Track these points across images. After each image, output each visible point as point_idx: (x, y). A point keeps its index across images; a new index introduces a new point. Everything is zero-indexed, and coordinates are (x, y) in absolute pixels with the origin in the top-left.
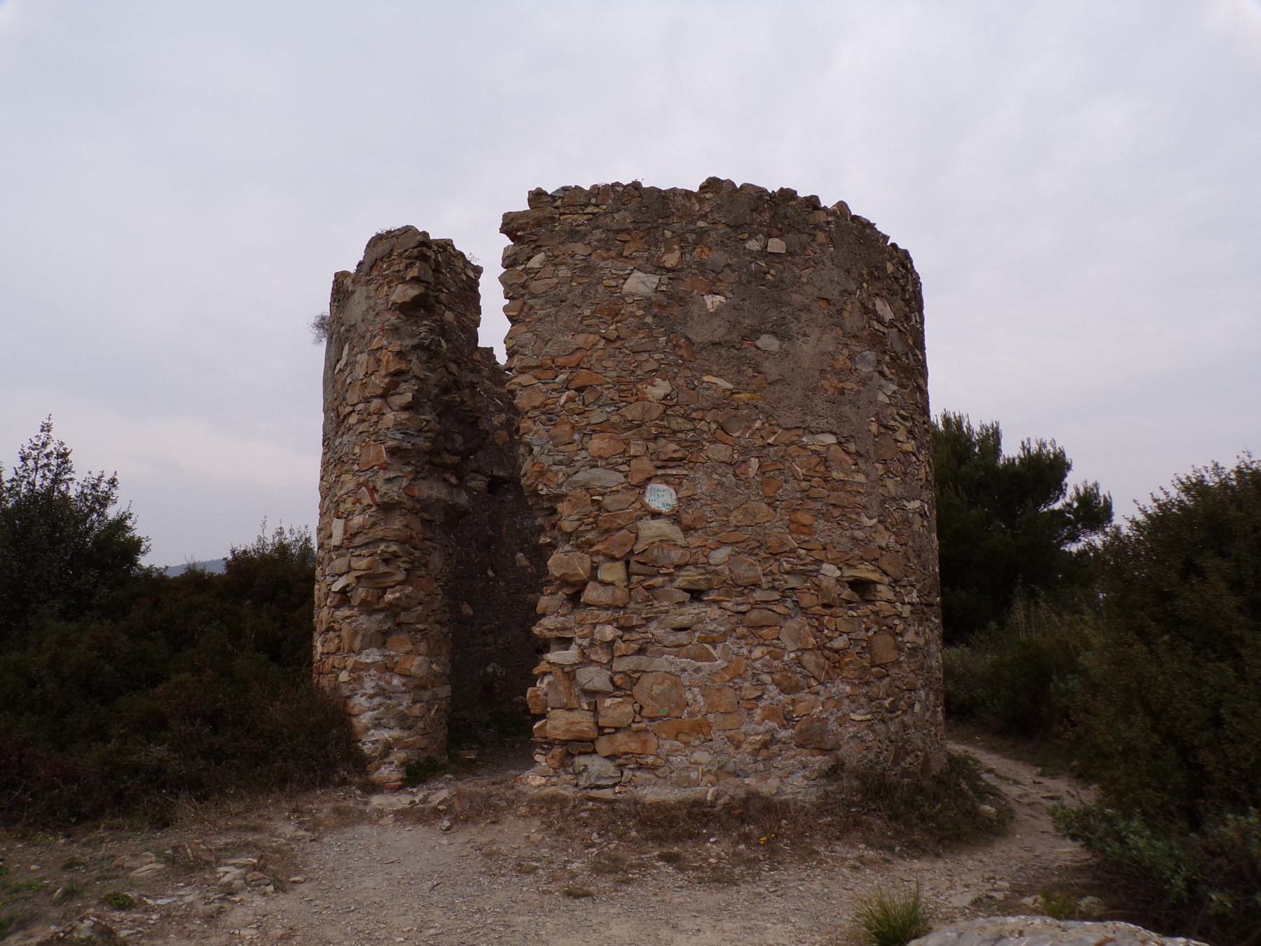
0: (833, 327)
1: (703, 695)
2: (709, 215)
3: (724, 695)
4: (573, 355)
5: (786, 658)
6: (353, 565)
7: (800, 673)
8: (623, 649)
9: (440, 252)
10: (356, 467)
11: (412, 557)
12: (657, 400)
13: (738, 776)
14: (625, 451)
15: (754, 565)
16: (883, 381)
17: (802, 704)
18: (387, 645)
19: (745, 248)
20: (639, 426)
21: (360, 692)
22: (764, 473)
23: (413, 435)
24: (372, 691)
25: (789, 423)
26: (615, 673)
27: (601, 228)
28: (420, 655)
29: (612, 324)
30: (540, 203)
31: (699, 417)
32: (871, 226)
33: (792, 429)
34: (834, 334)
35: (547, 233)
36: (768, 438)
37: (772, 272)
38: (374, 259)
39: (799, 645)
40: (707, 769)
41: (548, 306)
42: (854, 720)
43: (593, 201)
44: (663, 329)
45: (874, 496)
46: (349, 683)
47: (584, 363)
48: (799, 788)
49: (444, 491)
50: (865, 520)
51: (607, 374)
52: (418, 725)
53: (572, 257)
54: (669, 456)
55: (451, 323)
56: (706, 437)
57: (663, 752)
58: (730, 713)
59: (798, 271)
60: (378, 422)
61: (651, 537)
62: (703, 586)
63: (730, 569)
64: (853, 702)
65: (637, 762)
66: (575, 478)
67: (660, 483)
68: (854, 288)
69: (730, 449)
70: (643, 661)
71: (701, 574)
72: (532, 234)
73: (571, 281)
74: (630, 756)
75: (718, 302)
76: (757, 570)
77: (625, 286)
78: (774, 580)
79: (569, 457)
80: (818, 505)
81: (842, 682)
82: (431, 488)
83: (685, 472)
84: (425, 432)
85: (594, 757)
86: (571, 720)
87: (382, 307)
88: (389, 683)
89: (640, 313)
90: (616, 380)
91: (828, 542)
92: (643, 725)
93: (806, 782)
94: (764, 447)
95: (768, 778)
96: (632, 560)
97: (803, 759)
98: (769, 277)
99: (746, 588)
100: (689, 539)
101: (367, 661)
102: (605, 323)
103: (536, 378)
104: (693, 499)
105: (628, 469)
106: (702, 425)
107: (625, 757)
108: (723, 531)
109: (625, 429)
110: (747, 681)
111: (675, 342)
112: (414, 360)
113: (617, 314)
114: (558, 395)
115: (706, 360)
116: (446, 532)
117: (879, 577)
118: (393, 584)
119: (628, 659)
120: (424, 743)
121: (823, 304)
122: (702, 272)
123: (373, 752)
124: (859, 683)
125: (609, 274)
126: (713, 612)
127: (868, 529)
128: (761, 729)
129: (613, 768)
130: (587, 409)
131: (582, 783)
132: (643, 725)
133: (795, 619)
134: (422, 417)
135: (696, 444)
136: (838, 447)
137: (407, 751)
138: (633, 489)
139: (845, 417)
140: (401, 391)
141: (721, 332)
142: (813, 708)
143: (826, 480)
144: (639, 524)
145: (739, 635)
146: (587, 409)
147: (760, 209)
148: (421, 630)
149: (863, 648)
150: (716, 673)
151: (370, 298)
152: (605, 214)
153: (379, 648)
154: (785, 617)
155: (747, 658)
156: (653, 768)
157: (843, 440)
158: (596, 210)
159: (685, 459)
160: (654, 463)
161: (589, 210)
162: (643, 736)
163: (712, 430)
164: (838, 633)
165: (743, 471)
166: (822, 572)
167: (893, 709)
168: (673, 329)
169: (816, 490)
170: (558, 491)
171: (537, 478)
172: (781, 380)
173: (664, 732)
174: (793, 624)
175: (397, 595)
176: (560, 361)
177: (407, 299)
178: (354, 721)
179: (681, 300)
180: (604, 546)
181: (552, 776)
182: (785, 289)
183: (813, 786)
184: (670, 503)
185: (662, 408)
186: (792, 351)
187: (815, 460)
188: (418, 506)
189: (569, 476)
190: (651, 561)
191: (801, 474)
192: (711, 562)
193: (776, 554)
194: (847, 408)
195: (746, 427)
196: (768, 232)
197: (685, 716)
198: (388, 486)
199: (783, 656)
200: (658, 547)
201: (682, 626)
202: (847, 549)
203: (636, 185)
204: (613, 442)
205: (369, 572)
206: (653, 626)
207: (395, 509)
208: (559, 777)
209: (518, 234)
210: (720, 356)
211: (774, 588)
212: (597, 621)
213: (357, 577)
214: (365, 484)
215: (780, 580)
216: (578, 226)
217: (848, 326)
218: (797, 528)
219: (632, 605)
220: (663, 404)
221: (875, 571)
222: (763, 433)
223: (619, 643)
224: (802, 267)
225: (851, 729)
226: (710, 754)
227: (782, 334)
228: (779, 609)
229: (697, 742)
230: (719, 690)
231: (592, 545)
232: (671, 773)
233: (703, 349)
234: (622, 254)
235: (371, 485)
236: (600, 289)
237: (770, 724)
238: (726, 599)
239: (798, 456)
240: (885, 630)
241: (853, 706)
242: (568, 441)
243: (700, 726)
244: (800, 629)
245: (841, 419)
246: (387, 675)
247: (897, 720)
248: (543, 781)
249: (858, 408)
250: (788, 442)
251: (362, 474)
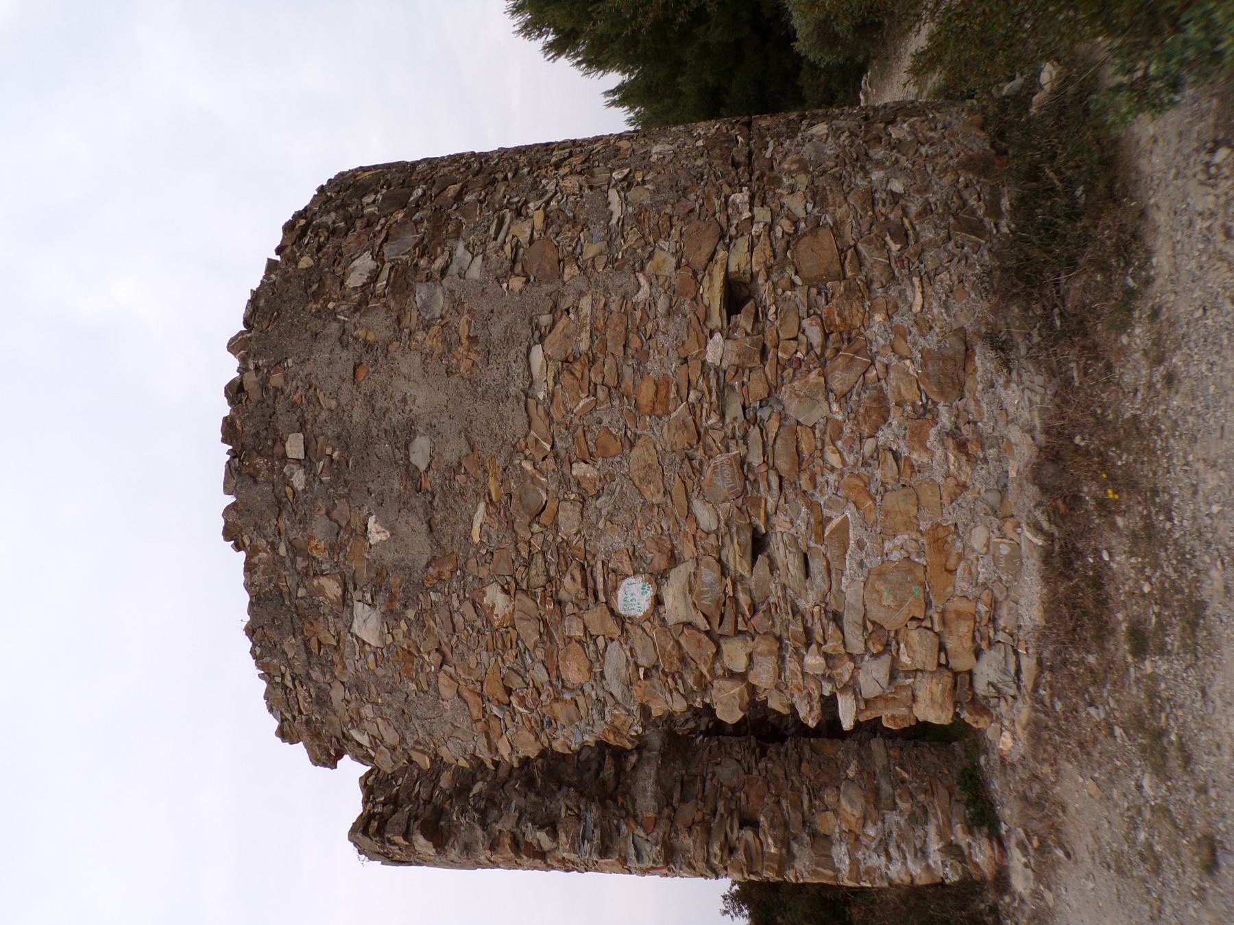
0: (389, 356)
1: (895, 536)
2: (270, 540)
3: (893, 506)
4: (468, 700)
5: (840, 417)
7: (859, 395)
8: (835, 644)
9: (374, 798)
11: (726, 815)
12: (511, 601)
13: (1006, 485)
14: (579, 642)
15: (715, 467)
16: (454, 269)
17: (903, 391)
18: (827, 833)
19: (304, 491)
20: (546, 624)
21: (884, 870)
22: (591, 455)
23: (584, 828)
24: (883, 859)
25: (521, 420)
26: (867, 649)
27: (308, 672)
28: (838, 800)
29: (423, 658)
31: (526, 547)
32: (256, 295)
33: (529, 416)
34: (398, 355)
36: (545, 450)
37: (329, 451)
39: (821, 397)
40: (996, 531)
42: (923, 306)
45: (608, 282)
48: (1023, 398)
49: (647, 769)
50: (642, 295)
53: (348, 702)
54: (580, 587)
55: (453, 774)
56: (551, 537)
57: (972, 592)
58: (918, 499)
59: (323, 414)
62: (747, 536)
63: (723, 502)
64: (896, 307)
65: (986, 625)
66: (619, 697)
67: (616, 598)
68: (335, 325)
69: (563, 504)
70: (851, 619)
73: (377, 704)
74: (977, 634)
75: (376, 525)
76: (722, 463)
77: (373, 644)
78: (733, 437)
79: (594, 704)
80: (628, 372)
81: (869, 327)
82: (645, 790)
83: (599, 565)
90: (491, 654)
91: (676, 355)
92: (936, 617)
93: (1013, 385)
94: (556, 457)
95: (1009, 440)
97: (980, 387)
98: (335, 455)
99: (746, 478)
102: (422, 666)
104: (634, 553)
105: (601, 638)
106: (537, 543)
108: (672, 513)
109: (551, 642)
110: (873, 474)
111: (435, 581)
113: (410, 653)
114: (518, 715)
115: (453, 539)
116: (694, 755)
117: (719, 265)
119: (848, 637)
120: (942, 792)
121: (361, 373)
122: (342, 547)
124: (869, 299)
125: (361, 662)
126: (781, 523)
127: (654, 291)
128: (939, 453)
129: (992, 652)
130: (531, 685)
131: (1012, 692)
132: (936, 617)
133: (786, 404)
134: (563, 815)
135: (563, 551)
136: (547, 340)
137: (953, 823)
138: (627, 631)
139: (505, 332)
141: (413, 520)
142: (908, 374)
143: (593, 361)
144: (671, 622)
145: (811, 486)
147: (252, 470)
148: (810, 800)
149: (819, 293)
150: (864, 518)
152: (290, 666)
153: (832, 844)
154: (783, 417)
155: (842, 475)
156: (994, 604)
157: (537, 334)
158: (288, 677)
159: (583, 565)
160: (592, 605)
161: (290, 684)
162: (950, 616)
163: (541, 529)
164: (801, 336)
165: (591, 485)
166: (718, 363)
167: (902, 235)
168: (418, 584)
169: (607, 376)
170: (637, 714)
172: (466, 433)
174: (793, 408)
175: (770, 841)
176: (476, 713)
177: (430, 844)
179: (381, 574)
181: (1002, 724)
182: (349, 433)
183: (1020, 375)
184: (641, 585)
185: (520, 596)
186: (427, 420)
187: (566, 378)
188: (666, 811)
189: (617, 703)
190: (718, 607)
191: (587, 400)
192: (714, 527)
193: (699, 433)
194: (493, 330)
195: (532, 482)
196: (279, 460)
198: (646, 859)
199: (837, 421)
200: (699, 599)
201: (802, 565)
202: (684, 324)
203: (250, 631)
204: (569, 656)
206: (802, 604)
210: (445, 520)
211: (745, 437)
215: (734, 428)
216: (310, 696)
217: (387, 334)
218: (660, 407)
219: (777, 631)
220: (515, 594)
221: (710, 275)
222: (539, 457)
223: (827, 648)
224: (318, 408)
225: (935, 311)
226: (975, 527)
227: (405, 435)
228: (773, 427)
229: (959, 544)
230: (886, 514)
232: (1000, 579)
233: (438, 544)
234: (335, 647)
237: (932, 439)
238: (763, 505)
239: (564, 404)
240: (792, 253)
241: (903, 308)
243: (936, 540)
244: (798, 396)
245: (509, 340)
247: (917, 228)
248: (1006, 734)
249: (492, 312)
250: (547, 422)
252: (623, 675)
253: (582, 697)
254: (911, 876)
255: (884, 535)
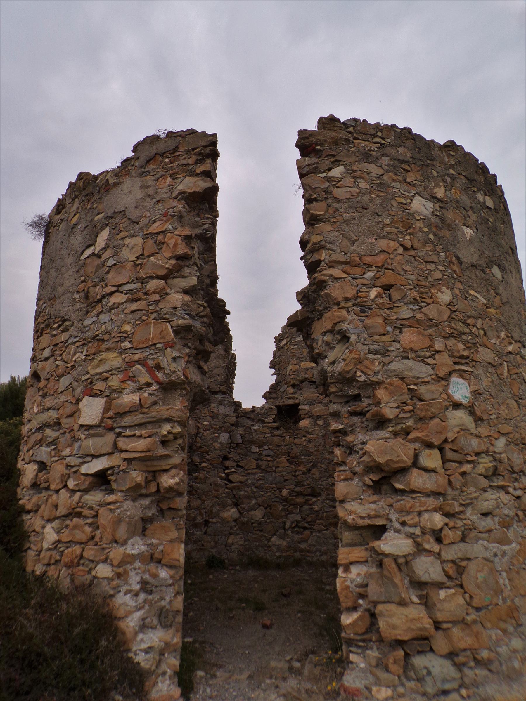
6: (122, 443)
10: (127, 345)
22: (511, 375)
30: (334, 127)
35: (345, 151)
38: (153, 153)
41: (352, 211)
43: (380, 134)
44: (441, 247)
46: (110, 580)
47: (388, 264)
51: (408, 277)
52: (176, 620)
53: (368, 174)
60: (159, 301)
61: (455, 426)
71: (491, 462)
72: (331, 149)
73: (370, 193)
83: (470, 369)
84: (202, 317)
85: (430, 655)
86: (411, 616)
87: (165, 196)
88: (155, 576)
89: (426, 229)
96: (447, 448)
100: (479, 429)
101: (133, 552)
103: (344, 272)
107: (463, 653)
109: (428, 326)
112: (196, 249)
113: (409, 228)
118: (168, 467)
119: (455, 547)
123: (152, 666)
125: (400, 193)
130: (395, 305)
140: (186, 275)
144: (447, 413)
146: (395, 305)
151: (148, 187)
158: (383, 142)
161: (377, 140)
170: (375, 379)
171: (355, 364)
173: (490, 621)
176: (368, 260)
178: (122, 625)
180: (423, 434)
184: (467, 395)
189: (385, 364)
197: (500, 602)
204: (420, 337)
205: (148, 454)
207: (175, 389)
208: (403, 685)
209: (318, 147)
212: (425, 508)
213: (125, 460)
214: (143, 362)
223: (446, 531)
231: (408, 434)
233: (467, 268)
234: (405, 180)
235: (151, 363)
236: (395, 204)
242: (383, 332)
246: (152, 567)
251: (136, 351)
252: (407, 373)
253: (390, 340)
254: (126, 616)
255: (509, 571)
